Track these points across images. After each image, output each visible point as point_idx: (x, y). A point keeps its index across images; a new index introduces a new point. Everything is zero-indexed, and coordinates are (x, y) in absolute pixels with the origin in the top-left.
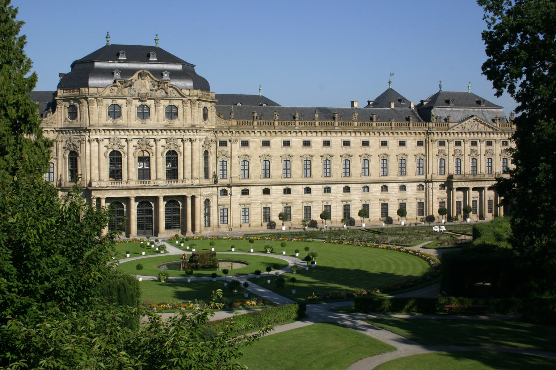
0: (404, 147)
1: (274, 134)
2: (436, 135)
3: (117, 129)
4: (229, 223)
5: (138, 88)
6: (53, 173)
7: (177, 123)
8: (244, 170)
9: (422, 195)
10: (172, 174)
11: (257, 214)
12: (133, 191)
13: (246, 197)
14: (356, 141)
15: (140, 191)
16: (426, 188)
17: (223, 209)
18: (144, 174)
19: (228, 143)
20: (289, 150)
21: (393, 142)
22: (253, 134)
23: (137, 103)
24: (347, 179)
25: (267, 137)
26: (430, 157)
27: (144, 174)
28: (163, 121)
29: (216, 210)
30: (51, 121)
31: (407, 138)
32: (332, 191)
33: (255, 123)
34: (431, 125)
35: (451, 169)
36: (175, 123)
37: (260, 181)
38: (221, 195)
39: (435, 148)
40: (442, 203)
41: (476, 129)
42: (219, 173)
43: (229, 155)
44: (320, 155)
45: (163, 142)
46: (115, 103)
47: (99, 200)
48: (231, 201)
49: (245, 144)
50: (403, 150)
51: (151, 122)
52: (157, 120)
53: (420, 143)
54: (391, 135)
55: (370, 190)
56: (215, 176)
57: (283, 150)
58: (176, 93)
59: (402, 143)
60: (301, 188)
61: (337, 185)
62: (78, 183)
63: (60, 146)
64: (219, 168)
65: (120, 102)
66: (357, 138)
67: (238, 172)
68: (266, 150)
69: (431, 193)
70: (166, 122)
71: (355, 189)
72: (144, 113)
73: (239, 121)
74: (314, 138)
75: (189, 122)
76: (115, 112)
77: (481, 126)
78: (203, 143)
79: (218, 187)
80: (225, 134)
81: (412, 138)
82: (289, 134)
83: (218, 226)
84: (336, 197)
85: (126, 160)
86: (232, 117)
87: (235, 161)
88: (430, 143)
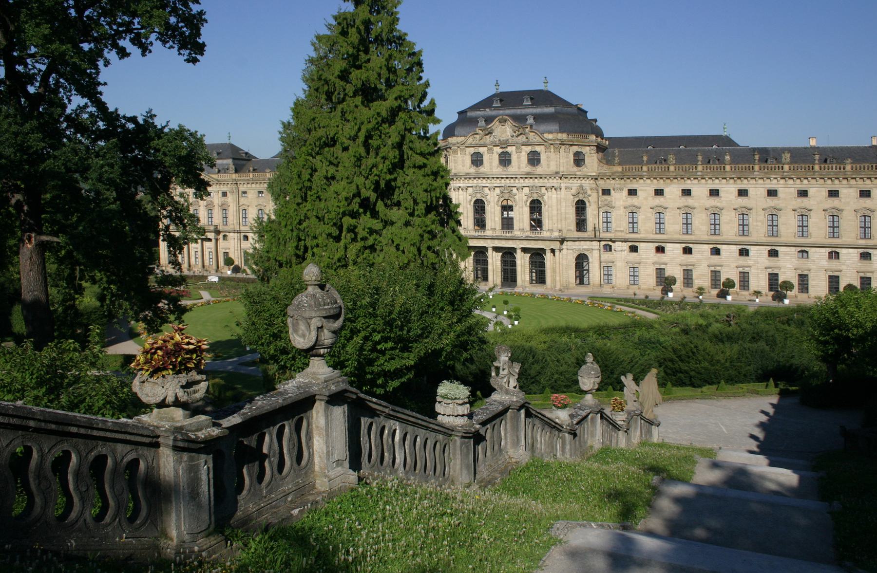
3: (478, 177)
5: (499, 134)
7: (539, 170)
14: (787, 190)
18: (508, 224)
19: (612, 192)
20: (689, 201)
28: (525, 168)
33: (645, 168)
49: (632, 192)
51: (513, 169)
65: (481, 150)
68: (659, 200)
70: (529, 169)
71: (786, 254)
72: (505, 160)
75: (553, 168)
76: (477, 160)
78: (574, 191)
84: (758, 263)
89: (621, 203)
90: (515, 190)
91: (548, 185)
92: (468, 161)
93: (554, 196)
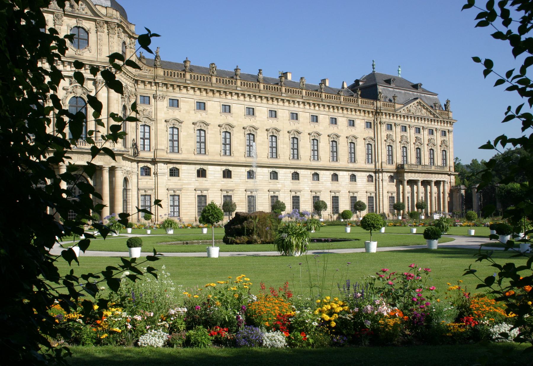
0: (353, 126)
1: (211, 94)
2: (384, 116)
9: (371, 187)
16: (376, 180)
17: (145, 195)
19: (152, 100)
20: (229, 119)
21: (342, 121)
22: (184, 91)
24: (295, 163)
25: (202, 97)
26: (379, 142)
29: (136, 196)
31: (355, 117)
32: (279, 177)
33: (188, 76)
34: (379, 104)
35: (398, 159)
36: (85, 54)
38: (142, 175)
39: (383, 132)
40: (392, 198)
41: (419, 114)
43: (153, 117)
48: (156, 184)
49: (174, 103)
50: (352, 131)
53: (369, 125)
54: (340, 111)
56: (135, 145)
58: (87, 10)
59: (352, 123)
61: (284, 170)
64: (140, 135)
66: (306, 111)
67: (165, 142)
68: (200, 116)
69: (381, 186)
73: (166, 71)
74: (259, 105)
77: (424, 111)
79: (138, 162)
80: (148, 86)
81: (361, 118)
82: (229, 97)
87: (162, 126)
88: (379, 125)
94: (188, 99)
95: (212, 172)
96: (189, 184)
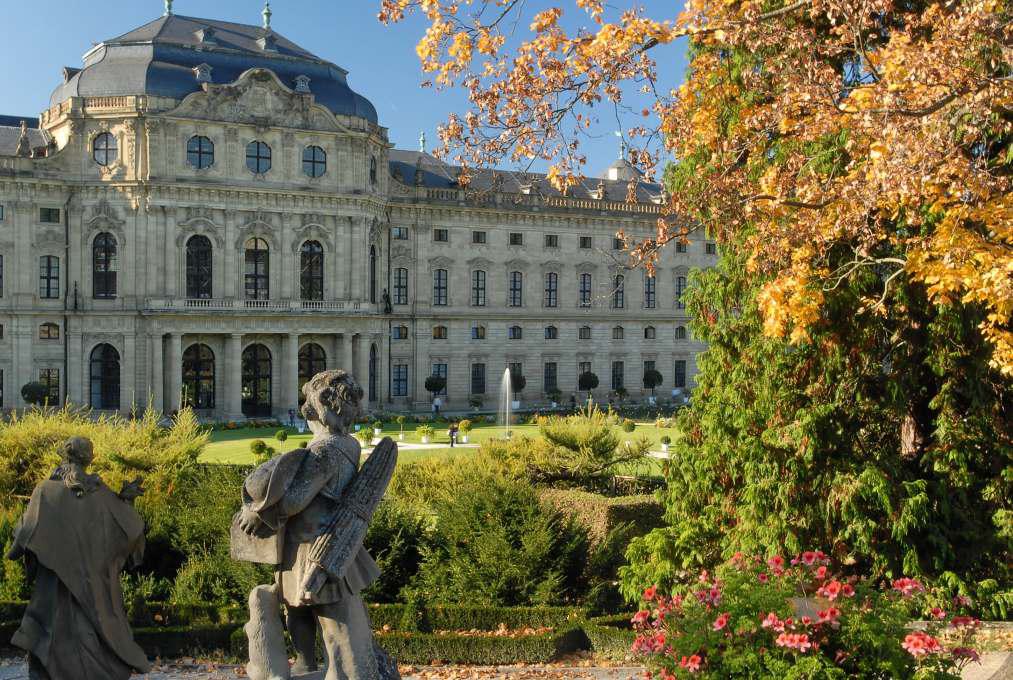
4: (409, 396)
6: (57, 278)
7: (324, 183)
8: (439, 288)
10: (312, 285)
11: (461, 376)
12: (238, 323)
13: (440, 343)
15: (253, 324)
18: (257, 283)
19: (411, 233)
20: (521, 253)
23: (248, 135)
27: (257, 283)
29: (387, 367)
30: (57, 165)
36: (322, 184)
37: (467, 310)
42: (393, 292)
44: (573, 263)
45: (297, 222)
46: (201, 133)
47: (167, 337)
49: (441, 236)
51: (274, 177)
52: (288, 176)
55: (657, 335)
57: (509, 252)
60: (540, 328)
62: (118, 302)
63: (75, 222)
64: (393, 282)
65: (213, 131)
67: (429, 292)
68: (478, 251)
70: (303, 180)
72: (259, 158)
75: (349, 182)
79: (391, 320)
83: (390, 401)
85: (222, 256)
86: (420, 180)
89: (426, 254)
90: (276, 221)
91: (341, 213)
92: (181, 154)
93: (348, 235)
94: (461, 227)
95: (494, 331)
96: (461, 348)
